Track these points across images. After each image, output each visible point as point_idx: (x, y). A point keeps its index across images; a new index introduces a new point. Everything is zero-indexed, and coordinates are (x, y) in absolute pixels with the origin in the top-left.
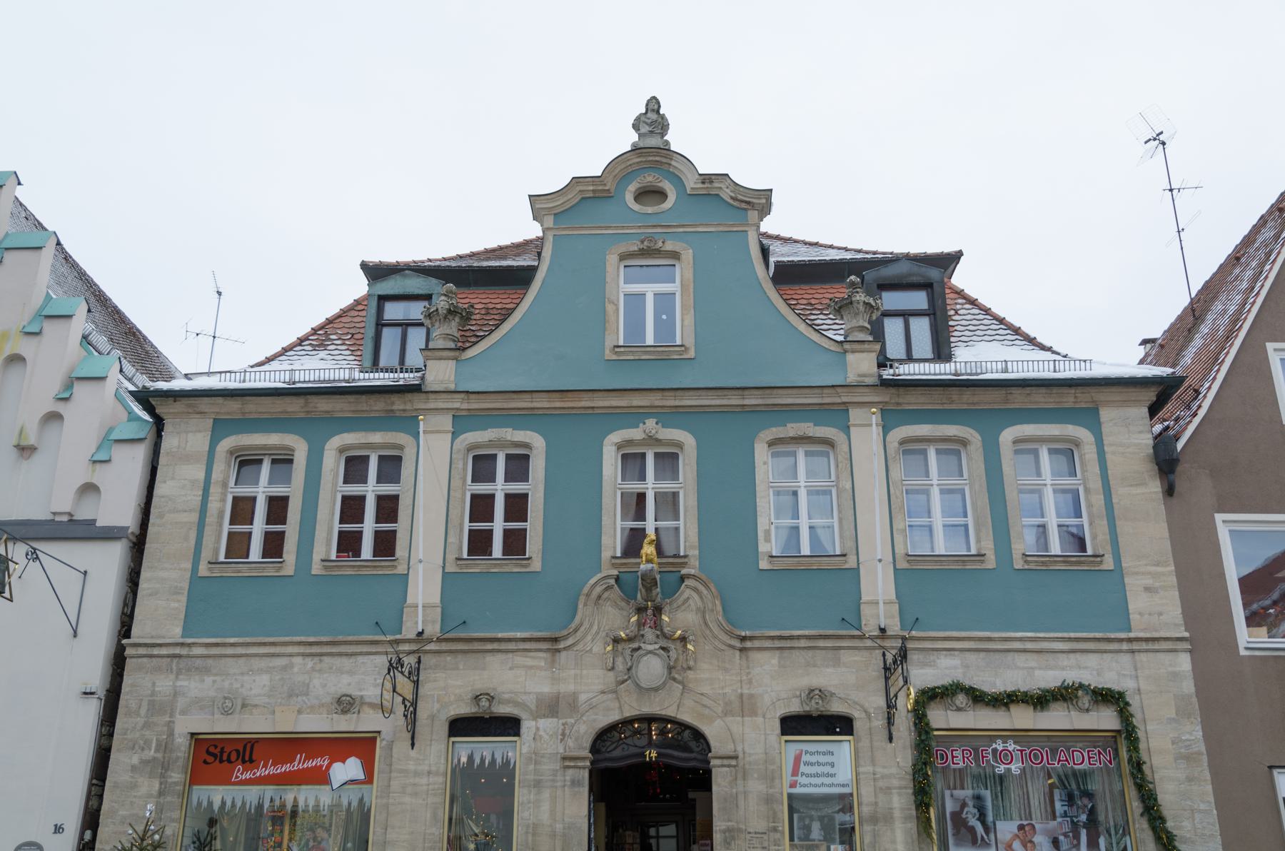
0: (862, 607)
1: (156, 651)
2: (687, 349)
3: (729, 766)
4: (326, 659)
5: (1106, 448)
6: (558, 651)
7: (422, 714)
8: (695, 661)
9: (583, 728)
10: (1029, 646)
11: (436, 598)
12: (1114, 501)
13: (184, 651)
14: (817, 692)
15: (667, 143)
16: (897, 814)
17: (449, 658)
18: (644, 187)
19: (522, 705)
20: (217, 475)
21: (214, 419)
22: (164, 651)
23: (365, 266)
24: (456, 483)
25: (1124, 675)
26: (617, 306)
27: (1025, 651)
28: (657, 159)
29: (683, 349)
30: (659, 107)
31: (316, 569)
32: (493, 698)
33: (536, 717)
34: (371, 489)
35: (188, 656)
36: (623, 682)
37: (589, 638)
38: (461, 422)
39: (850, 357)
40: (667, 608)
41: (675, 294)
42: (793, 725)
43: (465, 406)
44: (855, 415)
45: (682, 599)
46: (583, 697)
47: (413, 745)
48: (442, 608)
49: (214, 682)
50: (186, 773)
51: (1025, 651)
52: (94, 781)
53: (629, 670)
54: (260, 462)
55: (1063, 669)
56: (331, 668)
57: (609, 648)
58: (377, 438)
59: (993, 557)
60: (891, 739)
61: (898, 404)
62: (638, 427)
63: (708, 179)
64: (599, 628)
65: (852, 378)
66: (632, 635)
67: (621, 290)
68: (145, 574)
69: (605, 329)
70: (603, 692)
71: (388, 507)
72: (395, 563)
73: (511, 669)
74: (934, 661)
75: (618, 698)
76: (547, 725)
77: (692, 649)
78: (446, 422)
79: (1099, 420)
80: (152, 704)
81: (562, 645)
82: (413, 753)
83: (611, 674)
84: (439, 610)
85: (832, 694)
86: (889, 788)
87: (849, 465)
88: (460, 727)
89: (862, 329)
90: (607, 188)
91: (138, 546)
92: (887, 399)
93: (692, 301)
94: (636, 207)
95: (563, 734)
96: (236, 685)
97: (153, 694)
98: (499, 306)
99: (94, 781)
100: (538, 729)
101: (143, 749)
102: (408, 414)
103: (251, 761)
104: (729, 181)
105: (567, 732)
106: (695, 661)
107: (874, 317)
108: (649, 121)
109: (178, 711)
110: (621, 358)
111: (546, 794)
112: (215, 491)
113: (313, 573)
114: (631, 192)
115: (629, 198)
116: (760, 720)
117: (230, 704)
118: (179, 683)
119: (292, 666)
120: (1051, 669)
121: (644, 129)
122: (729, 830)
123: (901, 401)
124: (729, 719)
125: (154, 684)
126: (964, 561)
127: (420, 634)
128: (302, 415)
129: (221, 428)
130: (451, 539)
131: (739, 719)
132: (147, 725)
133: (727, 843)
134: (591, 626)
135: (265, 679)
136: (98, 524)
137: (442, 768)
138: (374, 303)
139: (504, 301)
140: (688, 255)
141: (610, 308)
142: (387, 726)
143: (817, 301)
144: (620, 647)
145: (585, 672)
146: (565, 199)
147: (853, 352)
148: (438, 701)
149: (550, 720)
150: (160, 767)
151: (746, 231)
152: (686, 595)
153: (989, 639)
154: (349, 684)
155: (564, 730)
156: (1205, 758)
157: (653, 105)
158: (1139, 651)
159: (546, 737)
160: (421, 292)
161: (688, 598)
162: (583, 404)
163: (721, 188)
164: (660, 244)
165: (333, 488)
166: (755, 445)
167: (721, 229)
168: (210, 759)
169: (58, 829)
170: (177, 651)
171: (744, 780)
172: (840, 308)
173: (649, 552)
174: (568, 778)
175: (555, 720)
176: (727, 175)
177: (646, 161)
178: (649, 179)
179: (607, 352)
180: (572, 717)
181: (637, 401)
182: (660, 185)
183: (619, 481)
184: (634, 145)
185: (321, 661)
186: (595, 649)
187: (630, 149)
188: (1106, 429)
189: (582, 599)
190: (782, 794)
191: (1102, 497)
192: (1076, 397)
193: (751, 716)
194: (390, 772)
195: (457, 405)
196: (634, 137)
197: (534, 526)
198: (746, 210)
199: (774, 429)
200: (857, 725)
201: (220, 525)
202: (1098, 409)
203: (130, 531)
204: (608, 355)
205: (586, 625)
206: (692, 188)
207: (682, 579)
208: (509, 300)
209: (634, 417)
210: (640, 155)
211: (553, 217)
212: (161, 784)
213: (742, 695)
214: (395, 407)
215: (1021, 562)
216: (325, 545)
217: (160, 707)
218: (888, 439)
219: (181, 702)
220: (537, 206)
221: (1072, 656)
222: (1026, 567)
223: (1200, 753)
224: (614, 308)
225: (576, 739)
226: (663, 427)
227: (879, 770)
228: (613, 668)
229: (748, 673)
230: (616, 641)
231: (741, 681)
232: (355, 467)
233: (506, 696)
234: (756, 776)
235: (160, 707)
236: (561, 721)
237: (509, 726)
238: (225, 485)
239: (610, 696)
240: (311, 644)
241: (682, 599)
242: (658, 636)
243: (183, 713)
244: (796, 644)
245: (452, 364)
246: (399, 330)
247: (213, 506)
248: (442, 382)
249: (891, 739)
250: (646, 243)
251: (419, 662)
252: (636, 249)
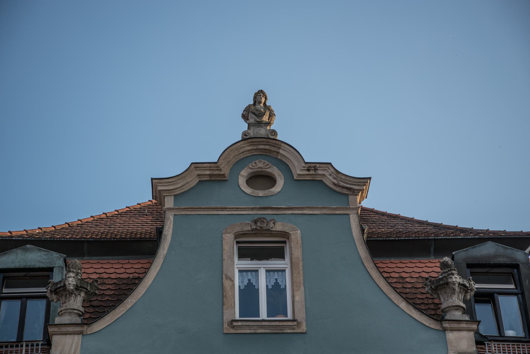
2: (299, 324)
15: (274, 132)
18: (257, 172)
26: (233, 281)
28: (267, 147)
29: (295, 323)
39: (451, 336)
41: (284, 271)
63: (312, 167)
67: (236, 266)
69: (223, 304)
89: (458, 307)
90: (222, 173)
93: (301, 278)
94: (248, 190)
98: (113, 276)
104: (332, 170)
107: (468, 297)
110: (239, 332)
114: (243, 176)
115: (242, 181)
121: (252, 119)
139: (117, 271)
140: (296, 235)
141: (227, 283)
143: (408, 275)
146: (185, 182)
147: (452, 330)
151: (348, 215)
160: (42, 265)
163: (324, 175)
164: (271, 225)
167: (325, 212)
172: (437, 287)
176: (330, 164)
177: (256, 149)
178: (260, 165)
179: (226, 325)
182: (269, 170)
184: (245, 134)
187: (240, 139)
196: (244, 126)
198: (347, 195)
204: (227, 329)
206: (299, 175)
208: (123, 270)
210: (252, 144)
211: (173, 198)
220: (159, 188)
224: (231, 283)
245: (77, 339)
246: (18, 304)
250: (259, 224)
252: (249, 228)
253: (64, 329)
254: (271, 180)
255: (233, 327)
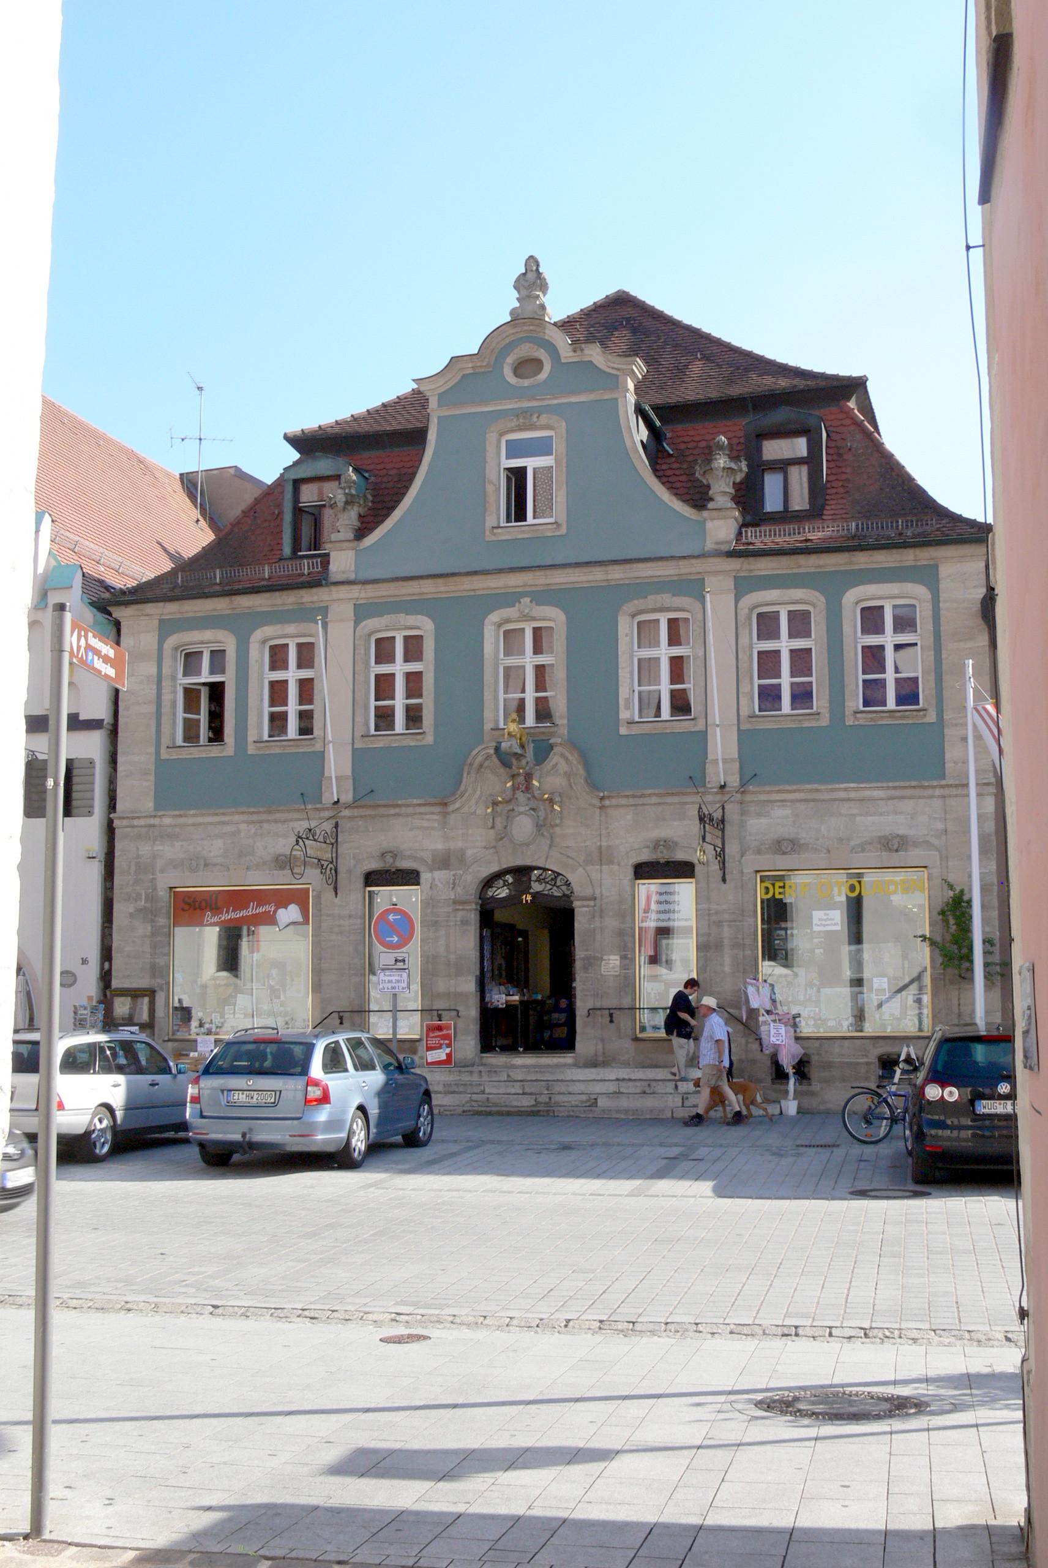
0: (707, 766)
1: (136, 822)
3: (588, 906)
4: (265, 825)
5: (941, 605)
6: (448, 813)
7: (342, 869)
8: (561, 819)
9: (469, 878)
10: (853, 795)
11: (348, 771)
12: (943, 656)
13: (156, 821)
14: (662, 843)
16: (726, 942)
17: (360, 823)
19: (422, 860)
20: (166, 671)
21: (160, 620)
22: (142, 822)
23: (287, 438)
24: (360, 667)
25: (935, 818)
27: (849, 800)
28: (532, 328)
29: (555, 526)
30: (538, 265)
31: (251, 750)
32: (396, 855)
33: (431, 870)
34: (292, 675)
35: (160, 826)
36: (501, 839)
37: (473, 801)
38: (362, 612)
40: (537, 774)
42: (643, 871)
43: (363, 595)
44: (711, 583)
45: (551, 764)
46: (469, 852)
47: (336, 894)
48: (354, 780)
49: (182, 845)
50: (170, 918)
51: (849, 800)
52: (106, 925)
53: (505, 828)
54: (202, 652)
55: (881, 814)
56: (269, 833)
57: (489, 810)
58: (291, 629)
59: (827, 715)
60: (724, 880)
61: (751, 571)
62: (514, 606)
64: (481, 793)
65: (710, 546)
66: (507, 798)
68: (120, 759)
69: (485, 511)
70: (485, 848)
71: (306, 689)
72: (313, 742)
73: (411, 830)
74: (768, 812)
75: (497, 852)
76: (441, 875)
77: (559, 809)
78: (348, 610)
79: (938, 574)
80: (138, 864)
81: (451, 808)
82: (337, 901)
83: (492, 831)
84: (351, 781)
85: (676, 844)
86: (720, 921)
87: (702, 634)
88: (372, 878)
91: (114, 732)
92: (738, 567)
94: (512, 380)
95: (454, 884)
96: (199, 849)
97: (138, 856)
99: (106, 925)
100: (434, 879)
101: (136, 901)
102: (316, 605)
103: (218, 909)
105: (457, 881)
106: (561, 819)
108: (527, 284)
109: (158, 869)
111: (442, 932)
112: (167, 684)
113: (250, 752)
116: (616, 867)
117: (198, 863)
118: (156, 848)
119: (239, 831)
120: (871, 816)
122: (587, 958)
123: (752, 567)
124: (589, 868)
125: (138, 848)
126: (800, 721)
127: (337, 802)
128: (229, 612)
129: (166, 628)
130: (358, 719)
131: (598, 867)
132: (136, 882)
133: (586, 968)
134: (474, 791)
135: (219, 843)
136: (81, 718)
137: (360, 913)
138: (289, 488)
141: (490, 488)
142: (312, 880)
144: (499, 809)
145: (470, 831)
148: (354, 858)
149: (444, 872)
150: (148, 913)
152: (554, 762)
153: (817, 791)
154: (284, 846)
155: (454, 880)
156: (996, 888)
157: (532, 263)
158: (950, 796)
159: (439, 884)
161: (557, 764)
162: (465, 587)
165: (262, 675)
166: (619, 618)
168: (186, 907)
169: (84, 961)
170: (152, 821)
171: (601, 917)
173: (512, 730)
174: (458, 919)
175: (447, 871)
178: (526, 350)
179: (487, 533)
180: (460, 869)
181: (515, 581)
183: (502, 656)
185: (261, 827)
186: (479, 812)
188: (943, 585)
189: (466, 769)
190: (633, 929)
191: (933, 653)
192: (916, 556)
193: (608, 864)
194: (321, 915)
195: (356, 595)
197: (427, 701)
199: (636, 602)
200: (698, 869)
201: (174, 714)
202: (935, 568)
203: (105, 722)
205: (470, 790)
207: (551, 747)
209: (509, 599)
212: (152, 927)
213: (601, 846)
214: (304, 600)
215: (852, 718)
216: (259, 726)
217: (144, 868)
218: (740, 605)
219: (159, 864)
221: (890, 802)
222: (857, 723)
223: (992, 885)
225: (464, 887)
226: (537, 604)
227: (713, 906)
228: (493, 827)
229: (607, 828)
230: (495, 804)
231: (600, 835)
232: (278, 657)
233: (408, 853)
234: (611, 914)
235: (144, 868)
236: (452, 873)
237: (410, 877)
238: (174, 678)
239: (491, 851)
240: (253, 813)
241: (551, 764)
242: (529, 799)
243: (162, 871)
244: (647, 800)
247: (167, 697)
248: (344, 572)
249: (724, 880)
251: (336, 826)
253: (338, 545)
254: (538, 363)
255: (494, 534)
